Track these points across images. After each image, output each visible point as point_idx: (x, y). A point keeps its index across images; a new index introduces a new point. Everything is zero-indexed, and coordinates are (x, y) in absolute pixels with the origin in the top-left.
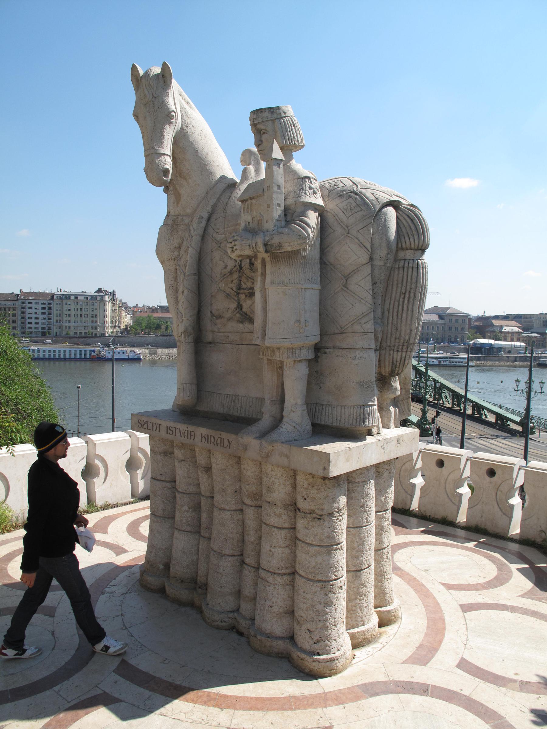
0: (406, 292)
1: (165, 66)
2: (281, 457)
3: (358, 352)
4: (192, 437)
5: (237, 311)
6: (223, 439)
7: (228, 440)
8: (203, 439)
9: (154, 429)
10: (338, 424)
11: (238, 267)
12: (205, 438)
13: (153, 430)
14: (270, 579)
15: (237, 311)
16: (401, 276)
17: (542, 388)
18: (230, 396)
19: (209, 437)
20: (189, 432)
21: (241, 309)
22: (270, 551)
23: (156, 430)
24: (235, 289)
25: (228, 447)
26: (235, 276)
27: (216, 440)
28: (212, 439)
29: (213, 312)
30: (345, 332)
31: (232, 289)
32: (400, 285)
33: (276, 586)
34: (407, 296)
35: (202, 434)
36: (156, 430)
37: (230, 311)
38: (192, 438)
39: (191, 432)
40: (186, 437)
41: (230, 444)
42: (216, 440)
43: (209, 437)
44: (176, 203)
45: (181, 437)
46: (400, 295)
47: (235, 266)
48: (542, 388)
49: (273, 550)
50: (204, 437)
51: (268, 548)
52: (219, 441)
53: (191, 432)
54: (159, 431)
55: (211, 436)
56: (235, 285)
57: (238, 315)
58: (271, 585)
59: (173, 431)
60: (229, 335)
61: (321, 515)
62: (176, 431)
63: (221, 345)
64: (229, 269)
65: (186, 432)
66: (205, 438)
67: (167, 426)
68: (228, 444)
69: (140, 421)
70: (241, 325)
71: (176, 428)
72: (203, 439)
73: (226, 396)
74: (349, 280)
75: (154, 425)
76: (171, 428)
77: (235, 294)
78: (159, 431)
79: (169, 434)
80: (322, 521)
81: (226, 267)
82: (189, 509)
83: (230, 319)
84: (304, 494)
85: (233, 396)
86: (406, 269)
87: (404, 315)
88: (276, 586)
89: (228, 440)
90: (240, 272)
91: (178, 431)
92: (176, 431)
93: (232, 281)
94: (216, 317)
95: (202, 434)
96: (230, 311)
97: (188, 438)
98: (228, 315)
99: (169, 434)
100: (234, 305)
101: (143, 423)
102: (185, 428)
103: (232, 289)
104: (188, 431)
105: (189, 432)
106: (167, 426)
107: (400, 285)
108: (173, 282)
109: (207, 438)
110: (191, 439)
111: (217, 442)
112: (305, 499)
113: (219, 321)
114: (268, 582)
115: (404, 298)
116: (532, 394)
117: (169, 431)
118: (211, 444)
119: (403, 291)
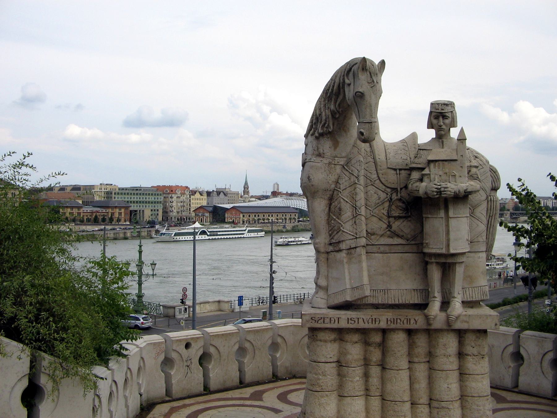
0: (492, 215)
1: (383, 63)
2: (462, 323)
3: (480, 253)
4: (377, 322)
5: (388, 229)
6: (410, 319)
7: (415, 319)
8: (389, 322)
9: (332, 322)
10: (471, 300)
11: (389, 197)
12: (391, 321)
13: (331, 323)
14: (451, 407)
15: (388, 229)
16: (489, 206)
17: (153, 270)
18: (383, 291)
19: (395, 319)
20: (374, 319)
21: (391, 228)
22: (448, 387)
23: (334, 323)
24: (386, 213)
25: (415, 323)
26: (387, 205)
27: (402, 321)
28: (399, 321)
29: (369, 231)
30: (473, 241)
31: (384, 214)
32: (489, 211)
33: (455, 409)
34: (493, 218)
35: (387, 319)
36: (334, 323)
37: (382, 229)
38: (377, 323)
39: (375, 319)
40: (370, 324)
41: (416, 322)
42: (402, 320)
43: (395, 319)
44: (333, 148)
45: (365, 324)
46: (489, 218)
47: (387, 197)
48: (153, 270)
49: (449, 386)
50: (390, 320)
51: (446, 385)
52: (405, 321)
53: (375, 319)
54: (338, 322)
55: (397, 319)
56: (386, 211)
57: (388, 233)
58: (452, 410)
59: (355, 321)
60: (380, 246)
61: (484, 355)
62: (358, 320)
63: (373, 254)
64: (382, 199)
65: (371, 320)
66: (391, 321)
67: (348, 318)
68: (415, 322)
69: (313, 318)
70: (391, 239)
71: (358, 318)
72: (389, 322)
73: (379, 291)
74: (474, 210)
75: (332, 319)
76: (352, 319)
77: (386, 217)
78: (338, 322)
79: (351, 323)
80: (484, 359)
81: (379, 198)
82: (360, 379)
83: (382, 236)
84: (473, 344)
85: (386, 291)
86: (492, 202)
87: (491, 229)
88: (455, 409)
89: (415, 319)
90: (390, 202)
91: (361, 320)
92: (358, 320)
93: (384, 209)
94: (371, 234)
95: (387, 319)
96: (382, 229)
97: (372, 323)
98: (381, 233)
99: (351, 323)
100: (385, 226)
101: (317, 320)
102: (370, 317)
103: (384, 214)
104: (372, 319)
105: (374, 319)
106: (348, 318)
107: (489, 211)
108: (325, 207)
109: (392, 321)
110: (375, 323)
111: (403, 321)
112: (473, 347)
113: (373, 237)
114: (449, 409)
115: (491, 219)
116: (143, 279)
117: (350, 321)
118: (397, 324)
119: (491, 215)
